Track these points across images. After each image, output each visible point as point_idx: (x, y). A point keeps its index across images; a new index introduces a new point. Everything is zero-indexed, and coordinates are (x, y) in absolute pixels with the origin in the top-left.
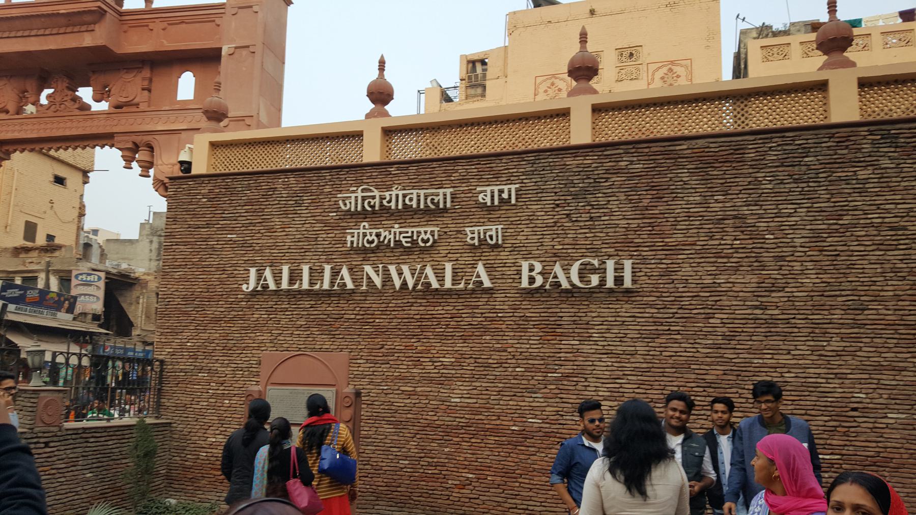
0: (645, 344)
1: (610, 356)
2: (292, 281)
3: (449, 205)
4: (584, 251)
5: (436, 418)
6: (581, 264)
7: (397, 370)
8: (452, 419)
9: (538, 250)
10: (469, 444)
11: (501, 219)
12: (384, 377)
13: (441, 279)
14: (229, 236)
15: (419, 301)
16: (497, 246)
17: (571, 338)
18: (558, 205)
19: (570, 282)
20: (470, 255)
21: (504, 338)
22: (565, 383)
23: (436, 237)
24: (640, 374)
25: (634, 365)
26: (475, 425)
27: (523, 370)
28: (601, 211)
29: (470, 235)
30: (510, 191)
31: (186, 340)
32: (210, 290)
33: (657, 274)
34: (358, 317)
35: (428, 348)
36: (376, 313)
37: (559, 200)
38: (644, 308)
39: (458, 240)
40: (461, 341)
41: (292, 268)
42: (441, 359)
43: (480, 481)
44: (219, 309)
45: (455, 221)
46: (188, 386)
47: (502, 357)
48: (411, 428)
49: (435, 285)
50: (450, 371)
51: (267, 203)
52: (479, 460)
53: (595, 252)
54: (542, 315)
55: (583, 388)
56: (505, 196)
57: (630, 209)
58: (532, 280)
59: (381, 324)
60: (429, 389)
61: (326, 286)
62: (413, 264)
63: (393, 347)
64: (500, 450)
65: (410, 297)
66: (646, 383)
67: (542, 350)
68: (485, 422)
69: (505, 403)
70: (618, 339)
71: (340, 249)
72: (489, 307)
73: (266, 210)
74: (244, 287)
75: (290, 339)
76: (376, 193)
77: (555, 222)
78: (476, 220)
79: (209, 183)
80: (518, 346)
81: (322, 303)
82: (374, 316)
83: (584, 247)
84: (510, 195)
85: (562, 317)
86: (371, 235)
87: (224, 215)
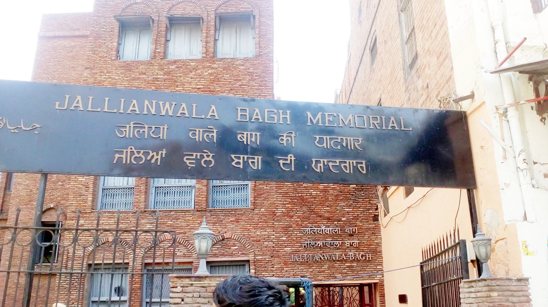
29: (347, 243)
30: (355, 229)
84: (355, 230)
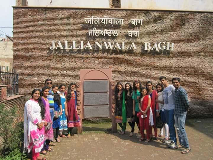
2: (69, 47)
6: (161, 43)
14: (41, 30)
18: (153, 27)
23: (119, 34)
32: (35, 49)
51: (56, 19)
53: (162, 40)
56: (139, 22)
58: (147, 47)
61: (82, 48)
76: (99, 19)
84: (141, 22)
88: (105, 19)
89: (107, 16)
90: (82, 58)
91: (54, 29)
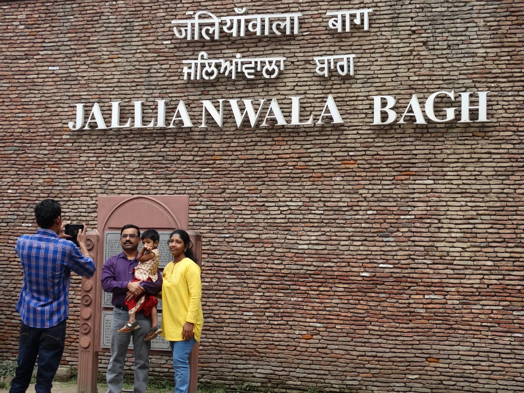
0: (500, 182)
1: (464, 195)
2: (122, 119)
3: (296, 32)
4: (441, 82)
5: (282, 267)
6: (437, 97)
7: (240, 216)
8: (299, 267)
9: (392, 81)
10: (317, 292)
11: (353, 47)
12: (226, 224)
13: (288, 115)
14: (50, 68)
15: (263, 140)
16: (348, 77)
17: (426, 178)
18: (414, 32)
19: (425, 116)
20: (320, 87)
21: (356, 178)
22: (418, 225)
23: (282, 68)
24: (494, 213)
25: (487, 204)
26: (323, 273)
27: (375, 212)
28: (459, 38)
29: (319, 66)
30: (362, 15)
31: (7, 187)
32: (32, 130)
33: (515, 106)
34: (197, 158)
35: (274, 192)
36: (216, 153)
37: (415, 26)
38: (500, 144)
39: (306, 71)
40: (309, 183)
41: (121, 104)
42: (288, 203)
43: (328, 330)
44: (41, 152)
45: (303, 50)
46: (11, 237)
47: (353, 200)
48: (256, 277)
49: (281, 121)
50: (297, 216)
51: (93, 30)
52: (327, 309)
53: (450, 83)
54: (396, 152)
55: (437, 230)
57: (489, 37)
58: (384, 116)
59: (223, 166)
60: (274, 236)
61: (161, 123)
62: (256, 98)
63: (235, 191)
64: (350, 297)
65: (254, 135)
66: (500, 222)
67: (395, 191)
68: (334, 269)
69: (356, 248)
70: (473, 178)
71: (175, 82)
72: (340, 145)
73: (91, 38)
74: (71, 125)
75: (123, 183)
76: (216, 20)
77: (411, 51)
78: (326, 48)
79: (27, 7)
80: (370, 187)
81: (157, 143)
82: (213, 157)
83: (441, 78)
84: (362, 20)
85: (416, 155)
86: (210, 66)
87: (44, 45)
88: (235, 18)
89: (244, 9)
90: (163, 156)
91: (84, 64)
